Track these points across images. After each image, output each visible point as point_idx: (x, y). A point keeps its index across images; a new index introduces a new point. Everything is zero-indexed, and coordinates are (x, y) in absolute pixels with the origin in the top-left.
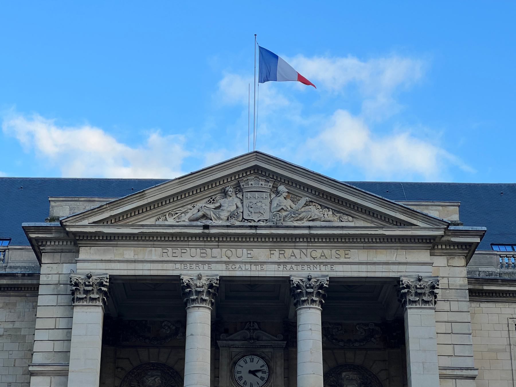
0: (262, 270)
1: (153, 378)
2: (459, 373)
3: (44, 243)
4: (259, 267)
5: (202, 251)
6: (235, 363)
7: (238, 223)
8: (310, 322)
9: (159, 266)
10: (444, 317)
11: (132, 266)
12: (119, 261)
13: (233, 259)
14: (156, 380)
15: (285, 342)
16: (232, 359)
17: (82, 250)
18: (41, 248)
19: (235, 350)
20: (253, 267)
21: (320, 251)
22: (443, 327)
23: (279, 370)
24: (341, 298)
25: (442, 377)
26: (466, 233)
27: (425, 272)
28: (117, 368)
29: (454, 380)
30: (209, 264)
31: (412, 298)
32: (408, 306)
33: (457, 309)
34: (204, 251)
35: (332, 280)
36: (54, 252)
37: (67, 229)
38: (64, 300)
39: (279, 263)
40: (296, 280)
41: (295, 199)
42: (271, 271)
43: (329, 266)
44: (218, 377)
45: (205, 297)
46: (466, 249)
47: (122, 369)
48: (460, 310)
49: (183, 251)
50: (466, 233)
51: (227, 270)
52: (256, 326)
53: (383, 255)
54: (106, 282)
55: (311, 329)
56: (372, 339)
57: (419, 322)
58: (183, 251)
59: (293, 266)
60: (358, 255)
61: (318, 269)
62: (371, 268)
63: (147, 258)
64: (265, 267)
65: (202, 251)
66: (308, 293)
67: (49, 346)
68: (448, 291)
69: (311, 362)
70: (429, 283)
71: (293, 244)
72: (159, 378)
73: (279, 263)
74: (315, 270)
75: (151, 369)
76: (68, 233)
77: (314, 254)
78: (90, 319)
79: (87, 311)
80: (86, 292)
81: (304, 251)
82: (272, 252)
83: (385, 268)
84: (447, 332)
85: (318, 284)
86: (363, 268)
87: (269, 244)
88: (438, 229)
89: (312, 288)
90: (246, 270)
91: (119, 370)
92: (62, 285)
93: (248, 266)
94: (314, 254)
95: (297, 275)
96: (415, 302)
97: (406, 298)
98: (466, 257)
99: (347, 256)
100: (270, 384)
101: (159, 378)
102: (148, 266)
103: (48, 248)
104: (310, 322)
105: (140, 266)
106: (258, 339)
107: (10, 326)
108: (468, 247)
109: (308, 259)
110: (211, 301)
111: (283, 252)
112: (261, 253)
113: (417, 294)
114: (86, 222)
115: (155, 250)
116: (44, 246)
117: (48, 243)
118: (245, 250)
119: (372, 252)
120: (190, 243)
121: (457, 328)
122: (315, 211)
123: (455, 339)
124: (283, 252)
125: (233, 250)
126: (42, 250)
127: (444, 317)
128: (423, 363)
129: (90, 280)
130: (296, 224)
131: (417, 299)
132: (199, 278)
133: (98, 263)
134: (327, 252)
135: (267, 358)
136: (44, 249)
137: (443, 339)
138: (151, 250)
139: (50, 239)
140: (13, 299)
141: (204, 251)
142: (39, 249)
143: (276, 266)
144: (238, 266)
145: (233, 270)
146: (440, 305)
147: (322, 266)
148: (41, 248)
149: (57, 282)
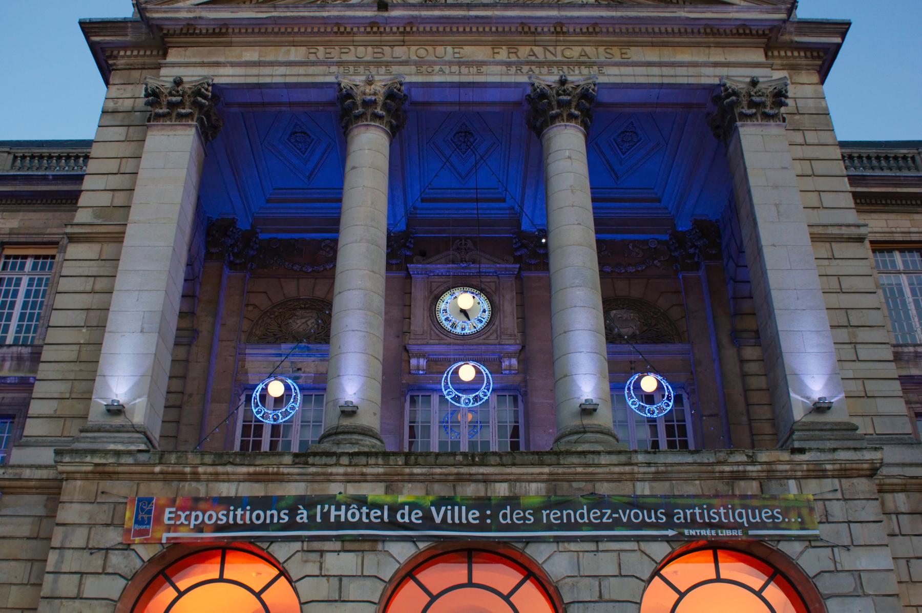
0: (479, 73)
1: (304, 320)
2: (835, 231)
3: (115, 53)
4: (474, 70)
5: (376, 50)
6: (437, 298)
9: (302, 70)
11: (254, 71)
12: (233, 64)
14: (309, 323)
15: (518, 266)
16: (431, 292)
17: (172, 51)
18: (110, 62)
19: (437, 279)
20: (464, 70)
21: (579, 48)
23: (509, 306)
28: (247, 305)
29: (828, 245)
30: (386, 66)
31: (746, 111)
32: (739, 123)
33: (816, 142)
34: (379, 50)
36: (130, 68)
37: (148, 15)
39: (508, 64)
43: (595, 68)
44: (410, 318)
45: (379, 111)
46: (819, 57)
47: (255, 306)
48: (822, 142)
49: (344, 50)
51: (419, 73)
52: (470, 244)
54: (207, 90)
55: (570, 158)
56: (656, 262)
58: (344, 50)
59: (533, 67)
61: (577, 72)
62: (666, 71)
63: (281, 58)
64: (484, 69)
65: (376, 50)
66: (561, 104)
67: (104, 199)
68: (797, 117)
69: (573, 206)
70: (771, 89)
71: (533, 38)
72: (313, 320)
73: (508, 64)
74: (572, 73)
75: (301, 308)
76: (148, 19)
77: (568, 53)
79: (170, 133)
80: (171, 105)
81: (551, 48)
82: (496, 50)
84: (805, 173)
85: (579, 90)
86: (655, 70)
87: (490, 38)
88: (777, 11)
89: (569, 95)
90: (451, 73)
91: (250, 308)
92: (138, 113)
93: (455, 69)
94: (568, 53)
96: (750, 116)
97: (733, 113)
98: (819, 72)
99: (624, 56)
100: (494, 328)
101: (313, 320)
102: (282, 70)
103: (121, 62)
105: (267, 70)
108: (821, 54)
110: (391, 122)
111: (514, 50)
113: (752, 104)
115: (296, 51)
116: (115, 58)
117: (122, 53)
118: (449, 49)
120: (355, 38)
121: (819, 167)
124: (514, 50)
125: (430, 48)
126: (112, 65)
128: (776, 205)
129: (180, 88)
131: (754, 111)
132: (370, 82)
135: (488, 290)
136: (115, 64)
138: (289, 51)
139: (125, 47)
141: (379, 50)
142: (107, 62)
143: (504, 68)
144: (437, 68)
145: (429, 73)
147: (583, 67)
148: (110, 62)
149: (129, 109)
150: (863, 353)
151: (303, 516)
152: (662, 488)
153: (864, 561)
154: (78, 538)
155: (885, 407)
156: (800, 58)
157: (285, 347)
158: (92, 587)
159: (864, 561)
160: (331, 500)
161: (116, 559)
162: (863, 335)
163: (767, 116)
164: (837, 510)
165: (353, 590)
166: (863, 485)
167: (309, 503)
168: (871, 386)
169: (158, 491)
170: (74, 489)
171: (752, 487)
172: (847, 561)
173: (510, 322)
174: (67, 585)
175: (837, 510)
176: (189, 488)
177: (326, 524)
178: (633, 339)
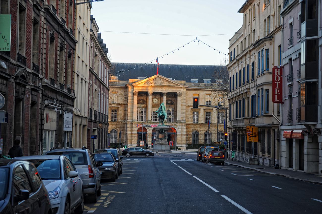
7: (156, 85)
8: (165, 98)
10: (182, 97)
13: (155, 89)
22: (182, 98)
23: (159, 100)
24: (169, 94)
25: (181, 105)
26: (186, 86)
27: (180, 91)
35: (168, 92)
38: (132, 94)
40: (163, 92)
41: (163, 81)
42: (160, 91)
50: (186, 86)
53: (175, 89)
57: (179, 97)
60: (172, 89)
78: (136, 97)
83: (175, 91)
86: (172, 91)
95: (163, 92)
104: (165, 98)
106: (156, 96)
107: (120, 93)
109: (165, 89)
112: (158, 89)
114: (135, 84)
119: (173, 88)
122: (166, 83)
123: (184, 100)
127: (182, 97)
130: (163, 85)
133: (137, 90)
134: (167, 88)
137: (182, 100)
140: (121, 89)
146: (182, 95)
150: (184, 114)
151: (147, 126)
152: (168, 125)
153: (180, 129)
154: (134, 127)
155: (184, 118)
156: (185, 88)
157: (140, 104)
158: (135, 130)
159: (180, 129)
160: (149, 125)
161: (137, 128)
162: (184, 113)
163: (180, 96)
164: (179, 126)
165: (150, 130)
166: (180, 124)
167: (147, 125)
168: (184, 117)
169: (138, 124)
170: (133, 124)
171: (174, 125)
172: (179, 129)
173: (159, 102)
174: (134, 130)
175: (179, 126)
176: (140, 124)
177: (148, 126)
178: (170, 104)
